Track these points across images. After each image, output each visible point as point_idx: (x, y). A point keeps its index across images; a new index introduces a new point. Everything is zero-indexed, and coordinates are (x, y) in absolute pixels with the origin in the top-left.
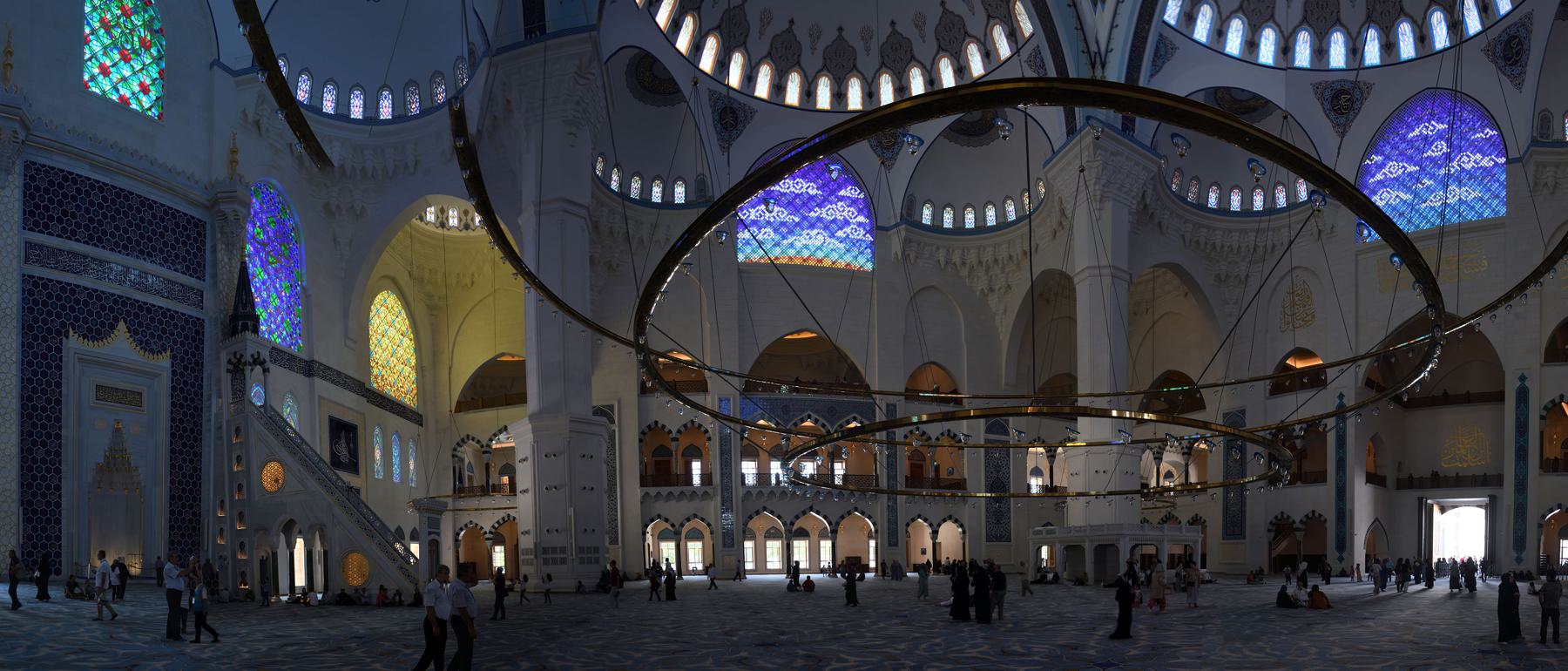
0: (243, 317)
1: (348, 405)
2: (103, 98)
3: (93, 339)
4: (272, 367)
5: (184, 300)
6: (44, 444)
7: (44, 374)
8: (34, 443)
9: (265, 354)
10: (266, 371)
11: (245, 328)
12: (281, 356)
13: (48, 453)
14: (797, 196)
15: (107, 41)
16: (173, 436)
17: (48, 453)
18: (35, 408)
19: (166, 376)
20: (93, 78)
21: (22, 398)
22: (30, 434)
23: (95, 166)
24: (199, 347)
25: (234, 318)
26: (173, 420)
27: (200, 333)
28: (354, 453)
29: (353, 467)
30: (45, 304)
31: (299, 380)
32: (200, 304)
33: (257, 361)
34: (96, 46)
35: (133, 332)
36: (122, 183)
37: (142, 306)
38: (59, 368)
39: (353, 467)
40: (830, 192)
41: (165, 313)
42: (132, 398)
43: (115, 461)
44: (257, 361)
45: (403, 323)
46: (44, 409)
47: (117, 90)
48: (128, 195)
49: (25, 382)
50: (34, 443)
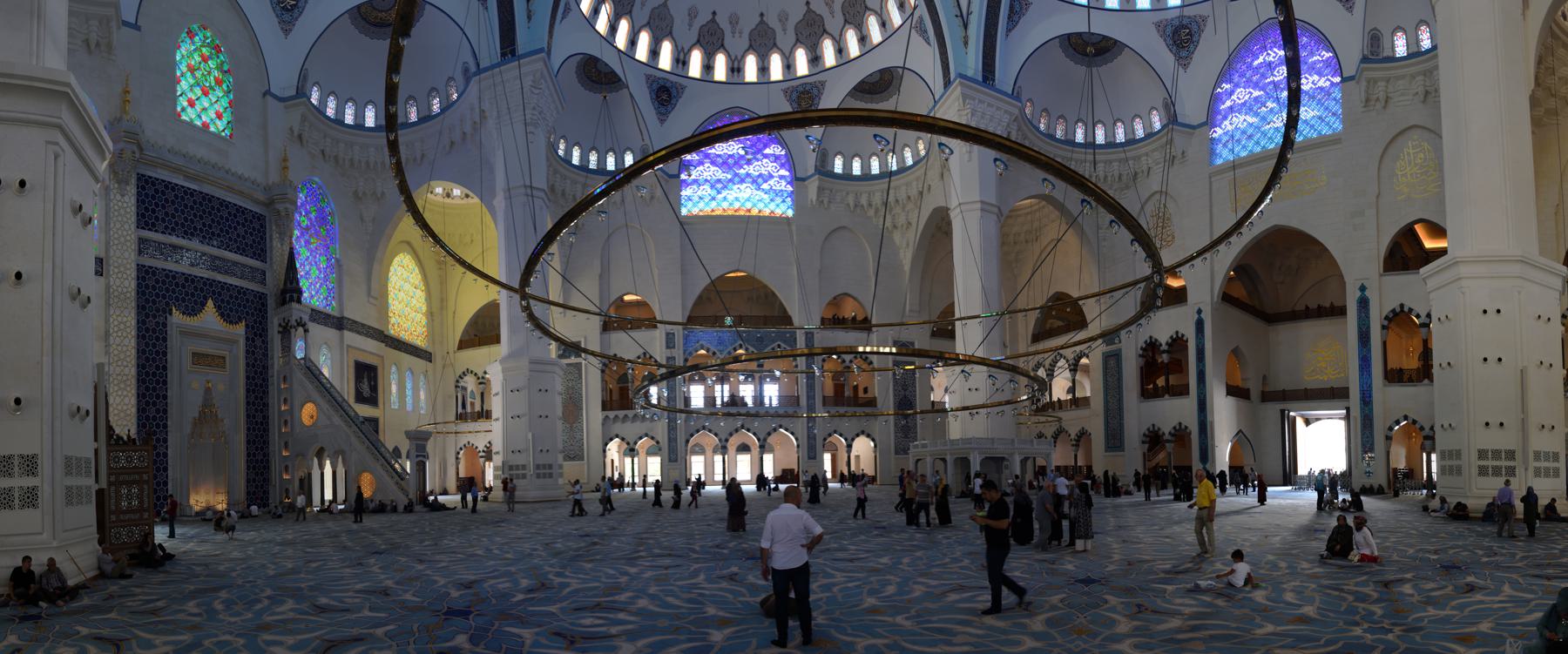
0: (290, 291)
1: (370, 349)
2: (190, 124)
3: (190, 315)
4: (312, 326)
5: (253, 279)
6: (154, 404)
7: (154, 345)
8: (147, 403)
9: (306, 318)
10: (306, 331)
11: (292, 300)
12: (319, 316)
13: (158, 411)
14: (731, 156)
15: (192, 81)
16: (248, 391)
19: (242, 342)
20: (183, 109)
22: (144, 396)
23: (187, 177)
24: (265, 317)
25: (284, 292)
26: (248, 378)
27: (264, 305)
28: (374, 389)
29: (372, 401)
30: (154, 288)
31: (331, 333)
32: (263, 282)
33: (301, 324)
35: (218, 308)
36: (207, 189)
37: (224, 286)
38: (165, 339)
39: (372, 401)
40: (757, 152)
41: (240, 290)
42: (216, 361)
43: (207, 415)
44: (301, 324)
45: (416, 277)
48: (211, 198)
49: (140, 352)
50: (147, 403)
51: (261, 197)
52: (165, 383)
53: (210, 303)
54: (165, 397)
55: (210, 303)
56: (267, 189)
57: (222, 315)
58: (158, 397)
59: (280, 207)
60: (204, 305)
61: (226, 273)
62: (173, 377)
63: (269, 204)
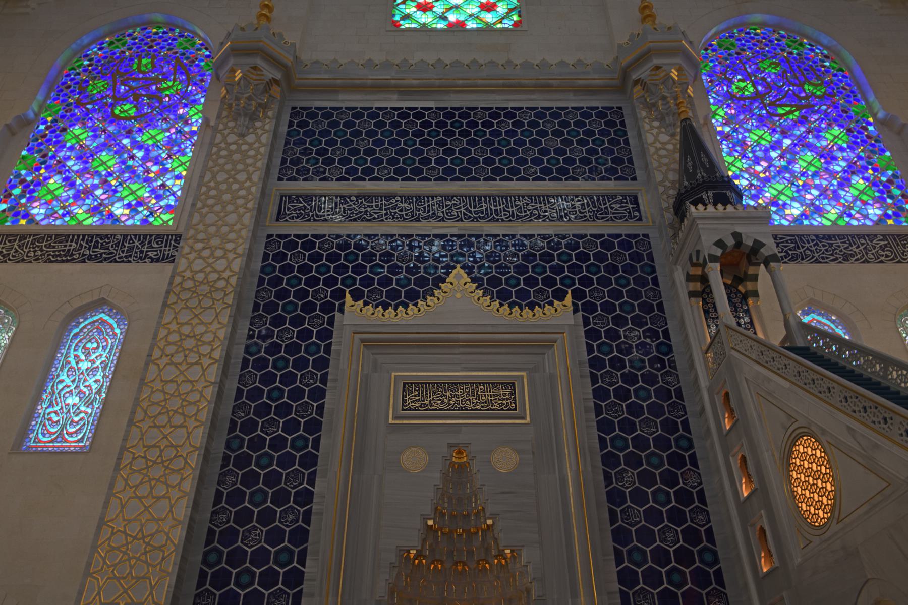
6: (266, 517)
13: (275, 537)
22: (236, 497)
47: (445, 18)
52: (310, 461)
53: (458, 276)
54: (306, 497)
57: (503, 296)
58: (281, 498)
62: (334, 445)
63: (623, 81)
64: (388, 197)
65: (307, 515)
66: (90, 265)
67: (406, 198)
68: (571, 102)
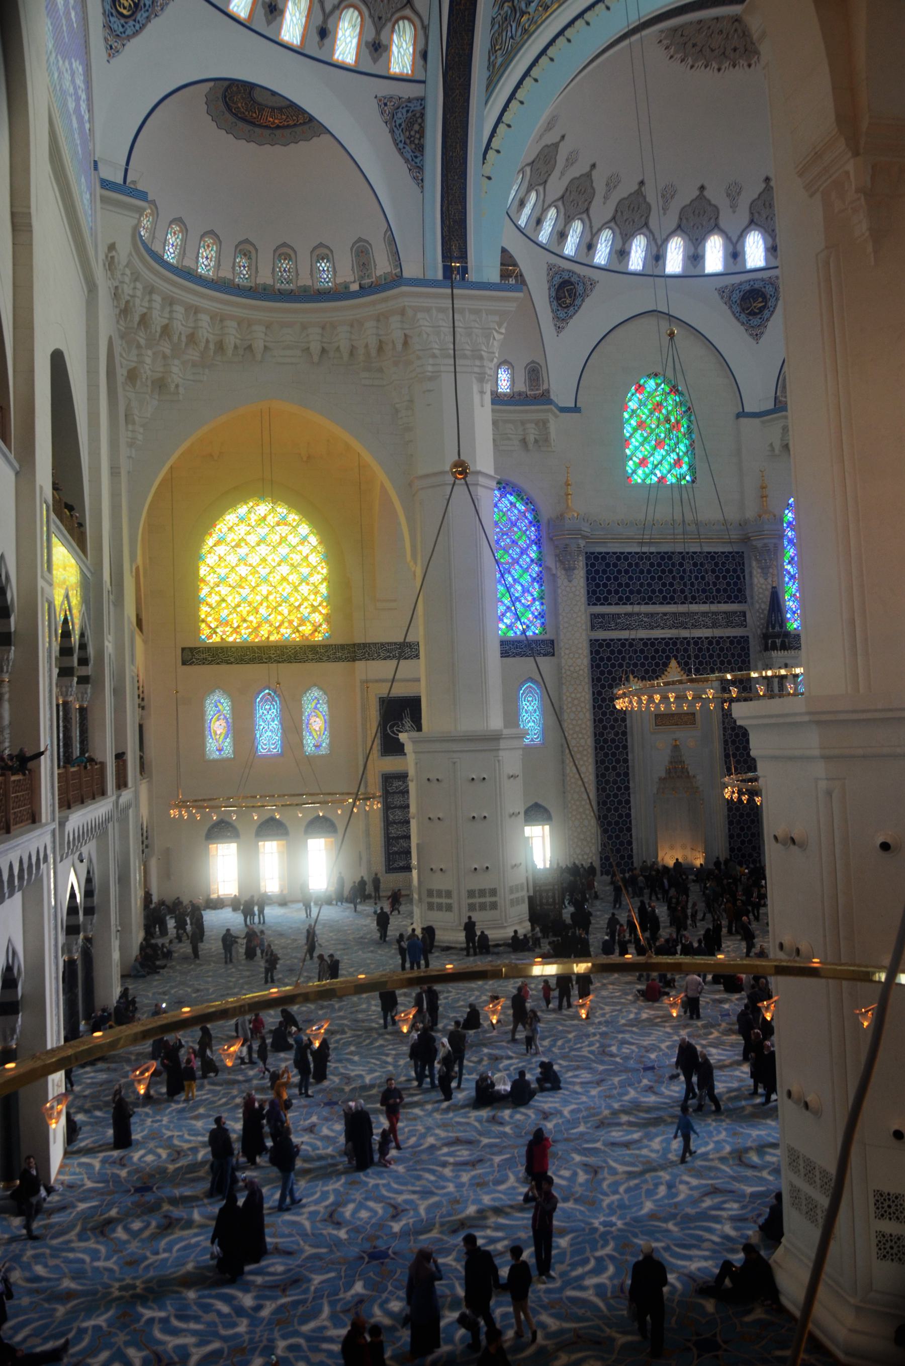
6: (614, 768)
8: (607, 769)
13: (618, 775)
17: (618, 775)
18: (605, 741)
21: (595, 735)
22: (603, 762)
34: (634, 442)
46: (613, 741)
50: (607, 769)
51: (735, 535)
53: (673, 663)
54: (626, 761)
55: (673, 663)
56: (743, 524)
58: (618, 761)
59: (759, 544)
60: (666, 665)
61: (694, 626)
64: (638, 614)
65: (628, 767)
66: (518, 659)
67: (647, 615)
68: (720, 549)
